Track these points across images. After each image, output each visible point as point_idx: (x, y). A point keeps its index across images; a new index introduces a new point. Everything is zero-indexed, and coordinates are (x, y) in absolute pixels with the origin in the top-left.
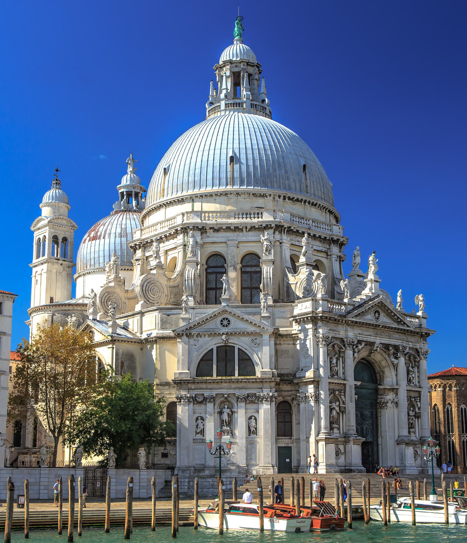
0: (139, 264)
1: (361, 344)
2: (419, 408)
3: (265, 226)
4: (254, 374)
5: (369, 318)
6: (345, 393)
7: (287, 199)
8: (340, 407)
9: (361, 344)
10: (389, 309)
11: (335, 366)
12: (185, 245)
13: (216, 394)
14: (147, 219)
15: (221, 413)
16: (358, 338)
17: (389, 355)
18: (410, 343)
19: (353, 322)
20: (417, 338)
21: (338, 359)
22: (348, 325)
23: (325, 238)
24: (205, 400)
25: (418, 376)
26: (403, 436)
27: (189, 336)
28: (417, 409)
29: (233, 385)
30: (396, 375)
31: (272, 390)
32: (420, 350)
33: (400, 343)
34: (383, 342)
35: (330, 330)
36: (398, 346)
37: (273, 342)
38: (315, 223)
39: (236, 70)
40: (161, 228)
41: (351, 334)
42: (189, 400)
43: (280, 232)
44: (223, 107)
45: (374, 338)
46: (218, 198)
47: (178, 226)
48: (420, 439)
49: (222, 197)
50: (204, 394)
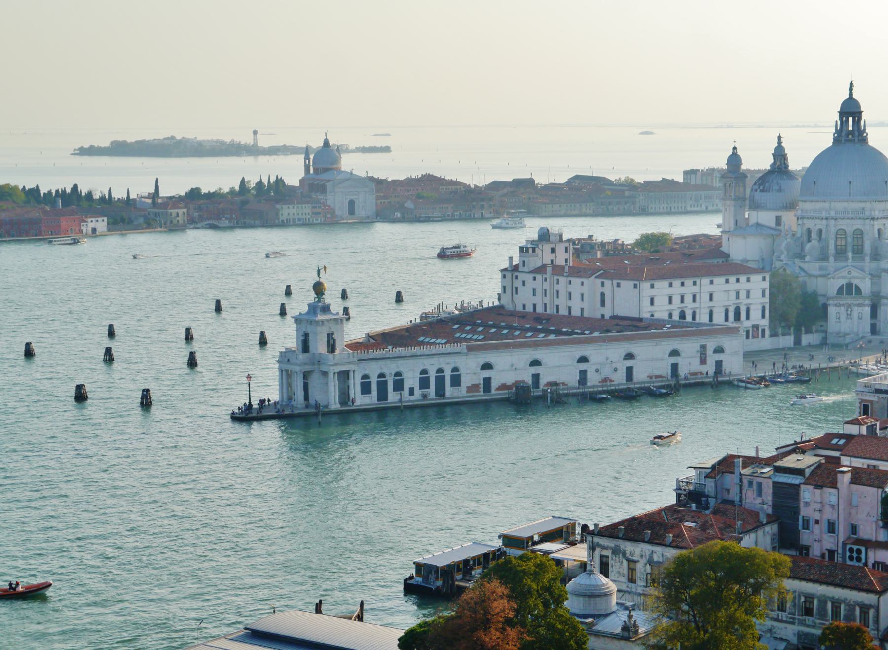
4: (861, 294)
15: (847, 310)
24: (840, 305)
27: (833, 278)
44: (843, 141)
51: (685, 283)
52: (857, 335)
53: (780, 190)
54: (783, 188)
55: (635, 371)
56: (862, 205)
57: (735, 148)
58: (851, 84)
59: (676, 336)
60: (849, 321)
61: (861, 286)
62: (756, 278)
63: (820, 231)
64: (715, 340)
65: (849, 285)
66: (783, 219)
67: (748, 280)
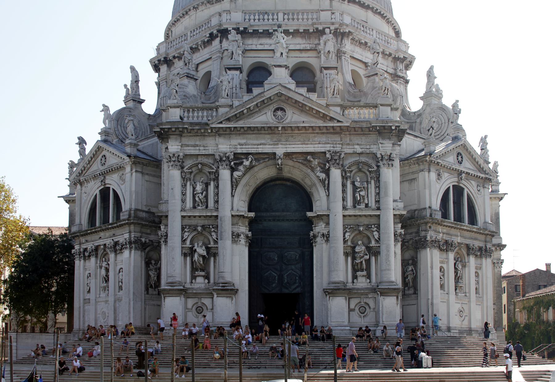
3: (208, 35)
11: (199, 193)
15: (101, 267)
16: (239, 151)
17: (313, 169)
20: (373, 137)
22: (220, 135)
29: (108, 233)
31: (132, 234)
33: (328, 149)
34: (289, 150)
38: (288, 15)
41: (225, 146)
42: (80, 255)
45: (272, 146)
46: (184, 19)
49: (187, 17)
60: (103, 295)
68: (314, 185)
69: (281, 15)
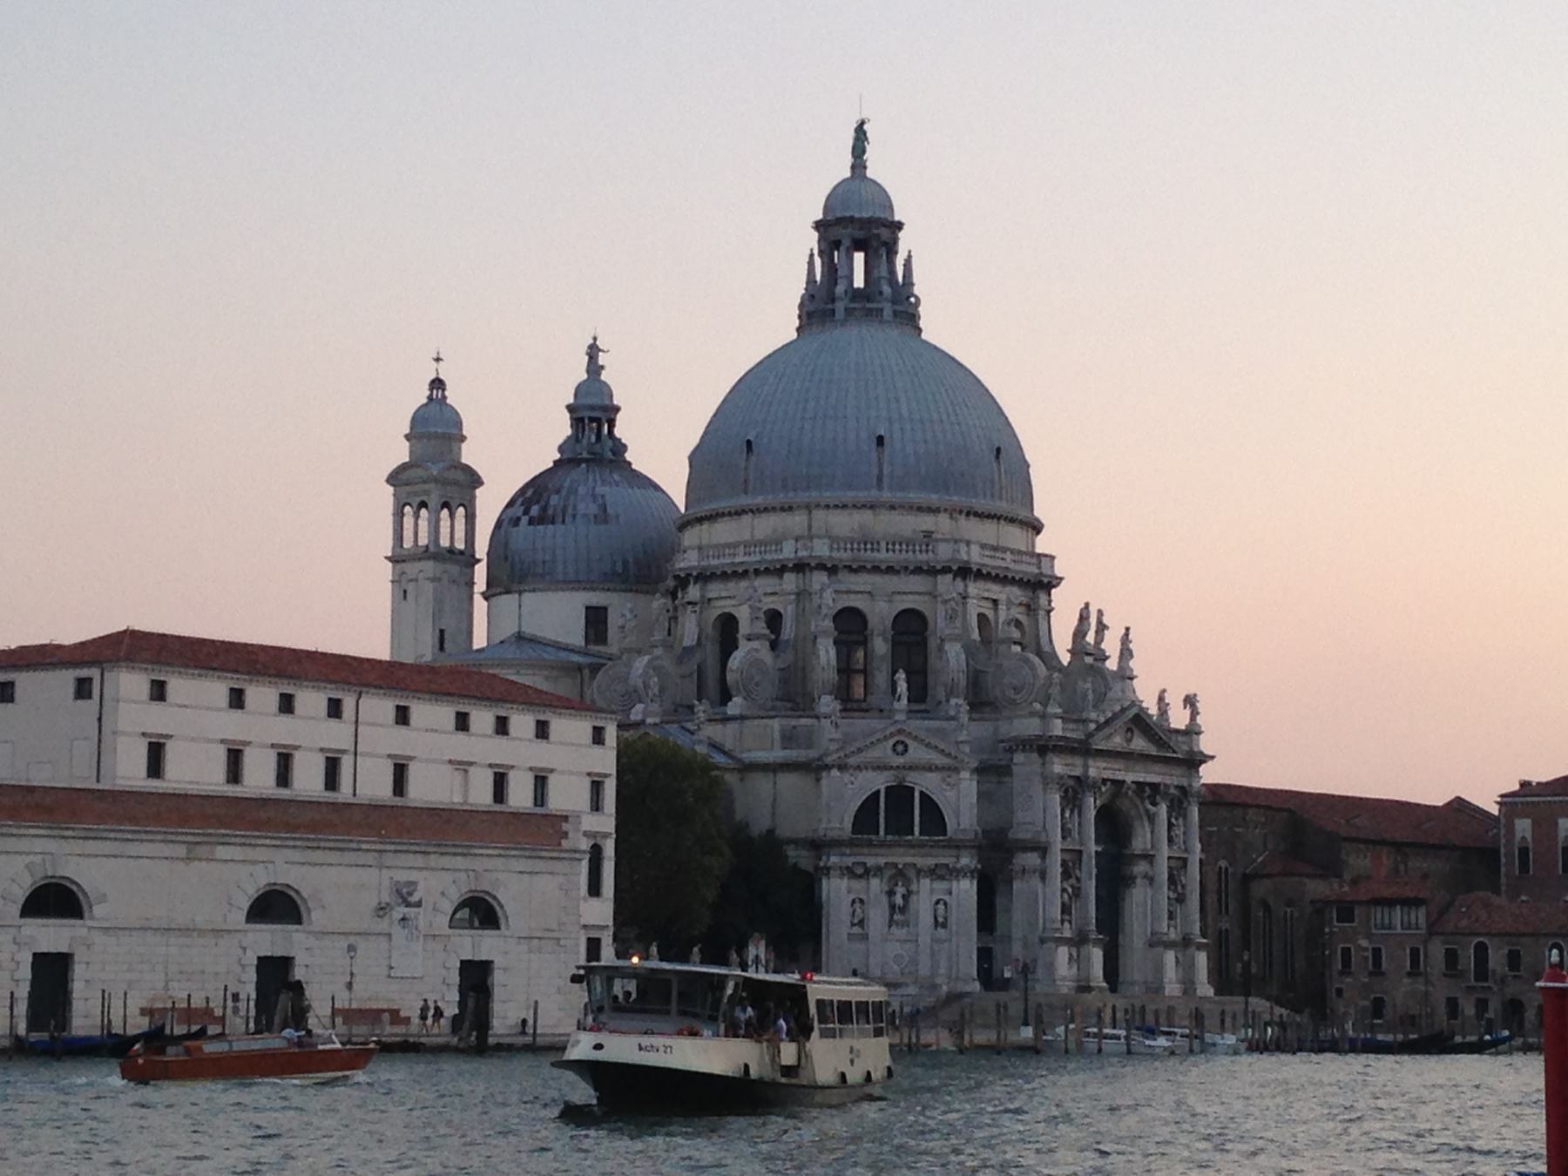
0: (695, 612)
1: (1105, 785)
2: (1183, 887)
4: (944, 832)
5: (1117, 742)
6: (1080, 865)
7: (972, 517)
8: (1072, 886)
9: (1105, 785)
10: (1148, 725)
12: (798, 594)
13: (886, 864)
14: (705, 526)
15: (891, 893)
18: (1175, 778)
19: (1097, 750)
21: (1072, 812)
23: (1029, 581)
24: (867, 873)
25: (1184, 833)
26: (1156, 933)
27: (842, 767)
28: (1179, 888)
30: (1152, 832)
32: (1188, 789)
35: (1066, 765)
36: (1159, 784)
37: (975, 783)
39: (860, 234)
40: (745, 554)
43: (964, 579)
46: (855, 511)
47: (788, 559)
48: (1184, 938)
50: (865, 864)
51: (299, 704)
52: (934, 987)
53: (603, 516)
54: (610, 511)
55: (79, 972)
56: (926, 522)
57: (437, 384)
58: (860, 134)
59: (291, 827)
61: (945, 799)
62: (571, 729)
63: (774, 619)
64: (459, 862)
65: (900, 795)
66: (614, 621)
67: (542, 730)
68: (1141, 818)
69: (1008, 553)
